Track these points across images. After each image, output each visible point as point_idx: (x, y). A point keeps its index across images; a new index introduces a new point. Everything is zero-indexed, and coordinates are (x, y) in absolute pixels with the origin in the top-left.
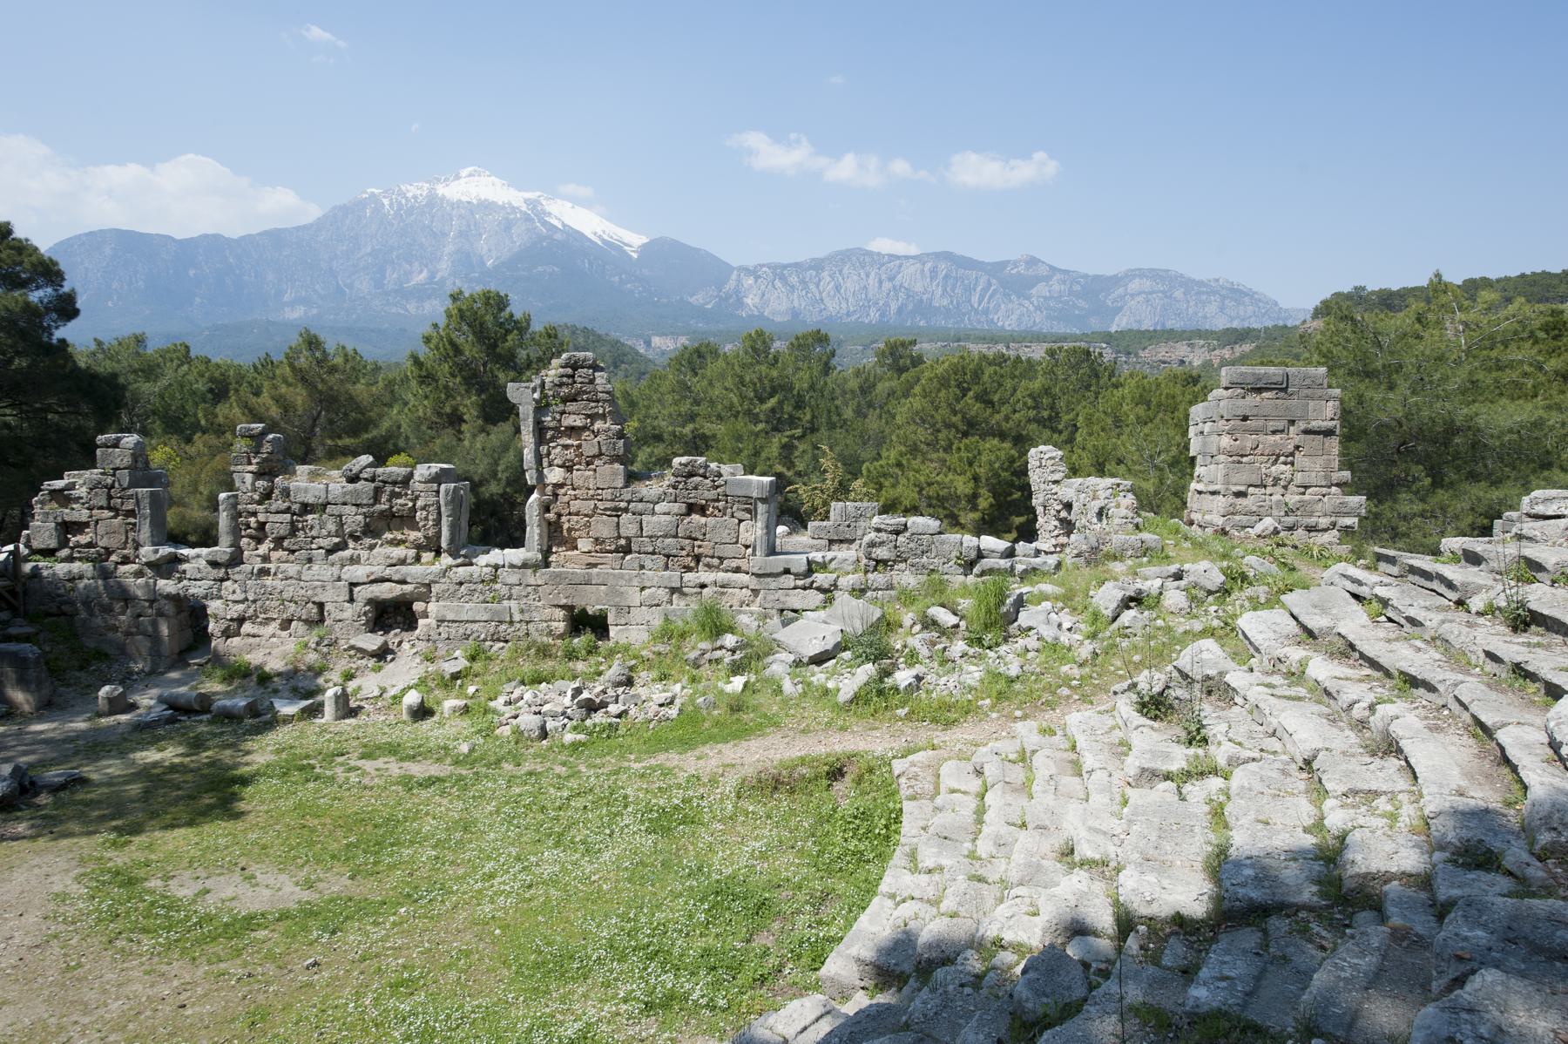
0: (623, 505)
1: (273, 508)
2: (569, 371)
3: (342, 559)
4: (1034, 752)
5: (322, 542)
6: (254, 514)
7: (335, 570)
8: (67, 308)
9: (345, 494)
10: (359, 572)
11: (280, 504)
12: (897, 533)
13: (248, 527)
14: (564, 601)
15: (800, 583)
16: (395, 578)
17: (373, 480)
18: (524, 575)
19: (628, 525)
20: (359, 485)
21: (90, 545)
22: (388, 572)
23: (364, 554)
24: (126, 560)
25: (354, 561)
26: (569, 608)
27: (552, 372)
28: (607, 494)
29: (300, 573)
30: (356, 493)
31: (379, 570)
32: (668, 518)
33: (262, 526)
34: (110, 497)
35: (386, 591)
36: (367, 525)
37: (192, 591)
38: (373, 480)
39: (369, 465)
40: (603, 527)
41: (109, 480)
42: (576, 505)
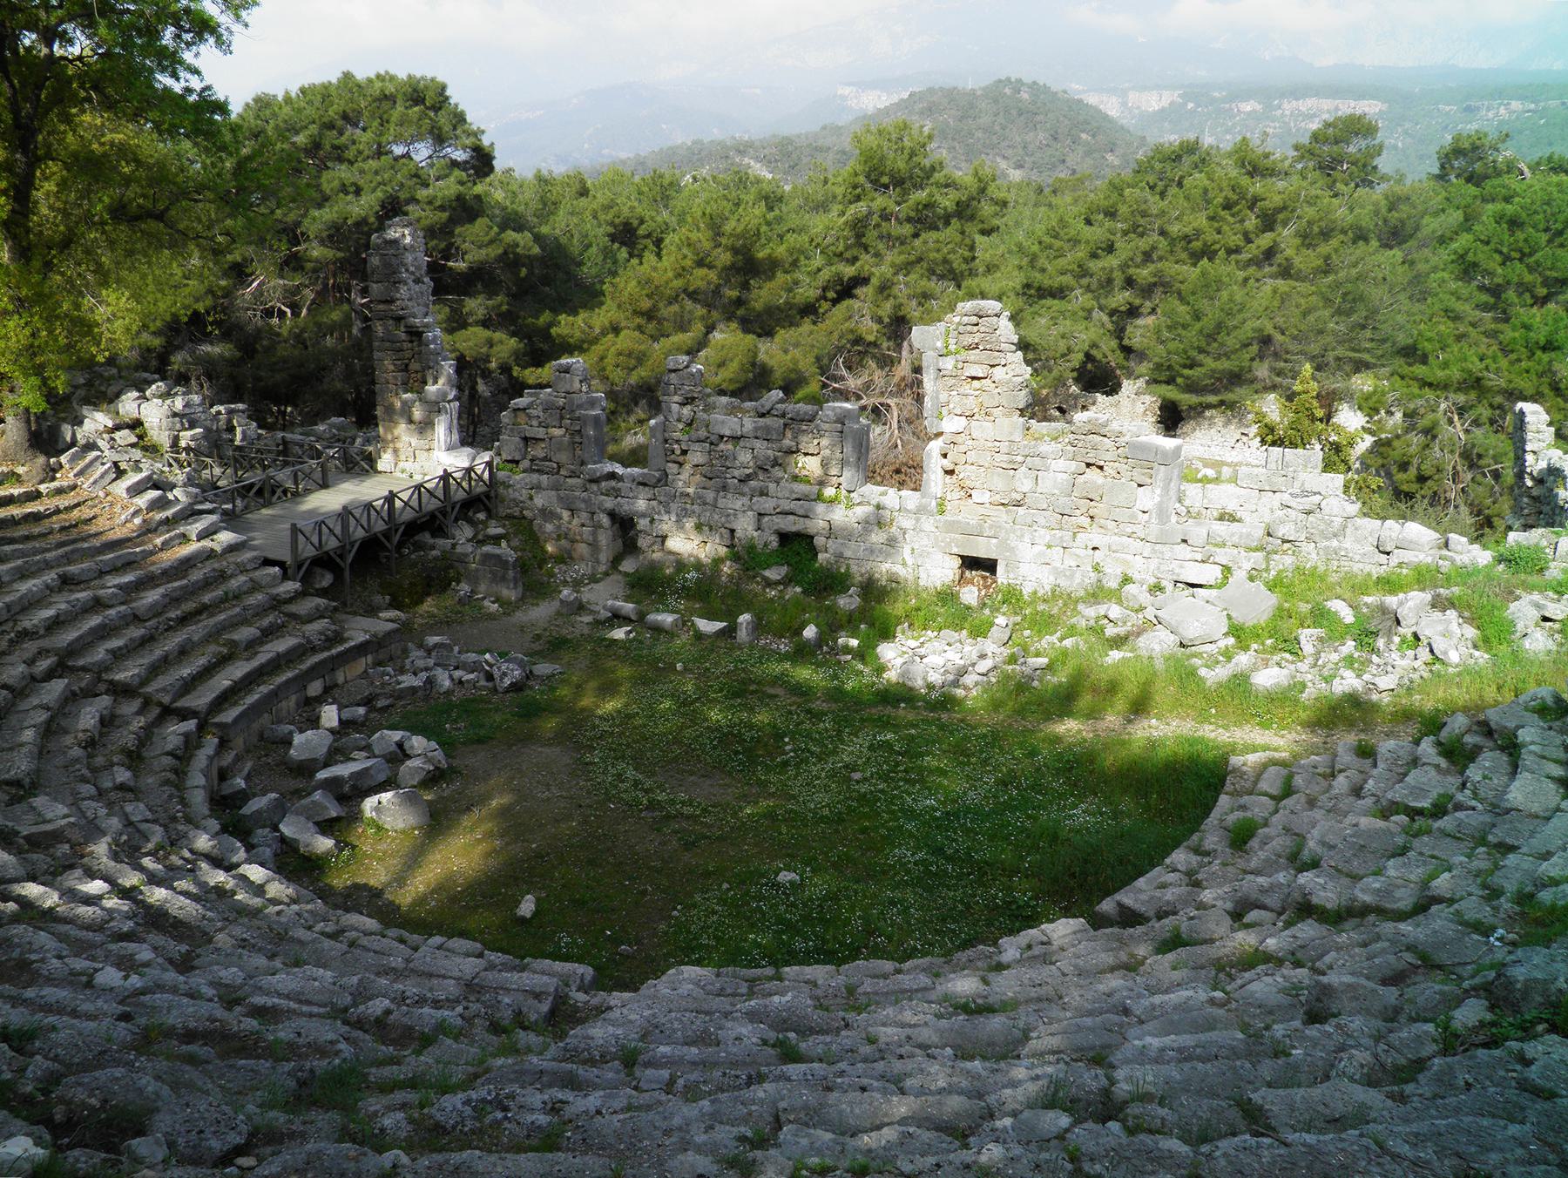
0: (1020, 459)
1: (694, 435)
2: (974, 319)
3: (753, 490)
4: (1341, 771)
5: (736, 473)
6: (678, 442)
7: (745, 500)
8: (482, 161)
9: (756, 429)
10: (767, 504)
11: (702, 433)
12: (1309, 513)
13: (673, 452)
14: (955, 550)
15: (1199, 557)
16: (801, 512)
17: (783, 415)
18: (918, 520)
19: (1024, 483)
20: (768, 421)
21: (545, 459)
22: (793, 506)
23: (772, 486)
24: (573, 475)
25: (763, 493)
26: (962, 557)
27: (957, 319)
28: (1004, 447)
29: (716, 499)
30: (767, 429)
31: (787, 505)
32: (1065, 476)
33: (684, 452)
34: (562, 418)
35: (790, 524)
36: (776, 459)
37: (626, 507)
38: (783, 415)
39: (781, 401)
40: (999, 483)
41: (561, 402)
42: (971, 456)
